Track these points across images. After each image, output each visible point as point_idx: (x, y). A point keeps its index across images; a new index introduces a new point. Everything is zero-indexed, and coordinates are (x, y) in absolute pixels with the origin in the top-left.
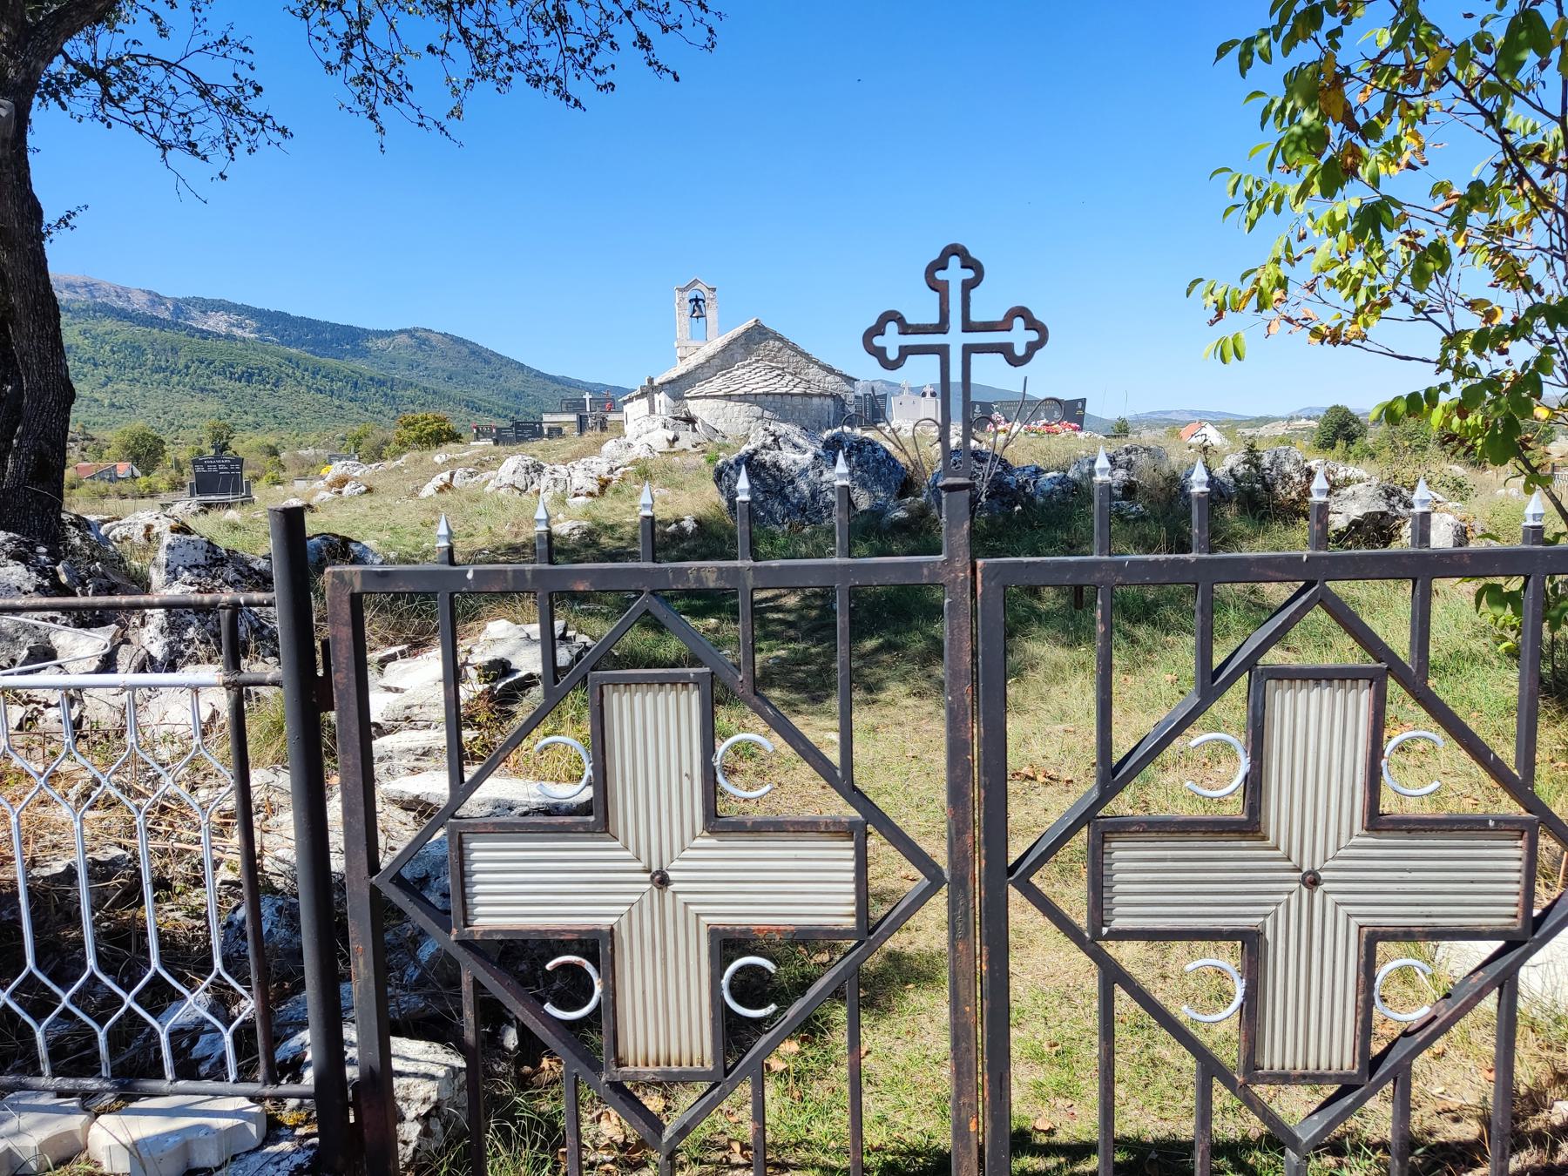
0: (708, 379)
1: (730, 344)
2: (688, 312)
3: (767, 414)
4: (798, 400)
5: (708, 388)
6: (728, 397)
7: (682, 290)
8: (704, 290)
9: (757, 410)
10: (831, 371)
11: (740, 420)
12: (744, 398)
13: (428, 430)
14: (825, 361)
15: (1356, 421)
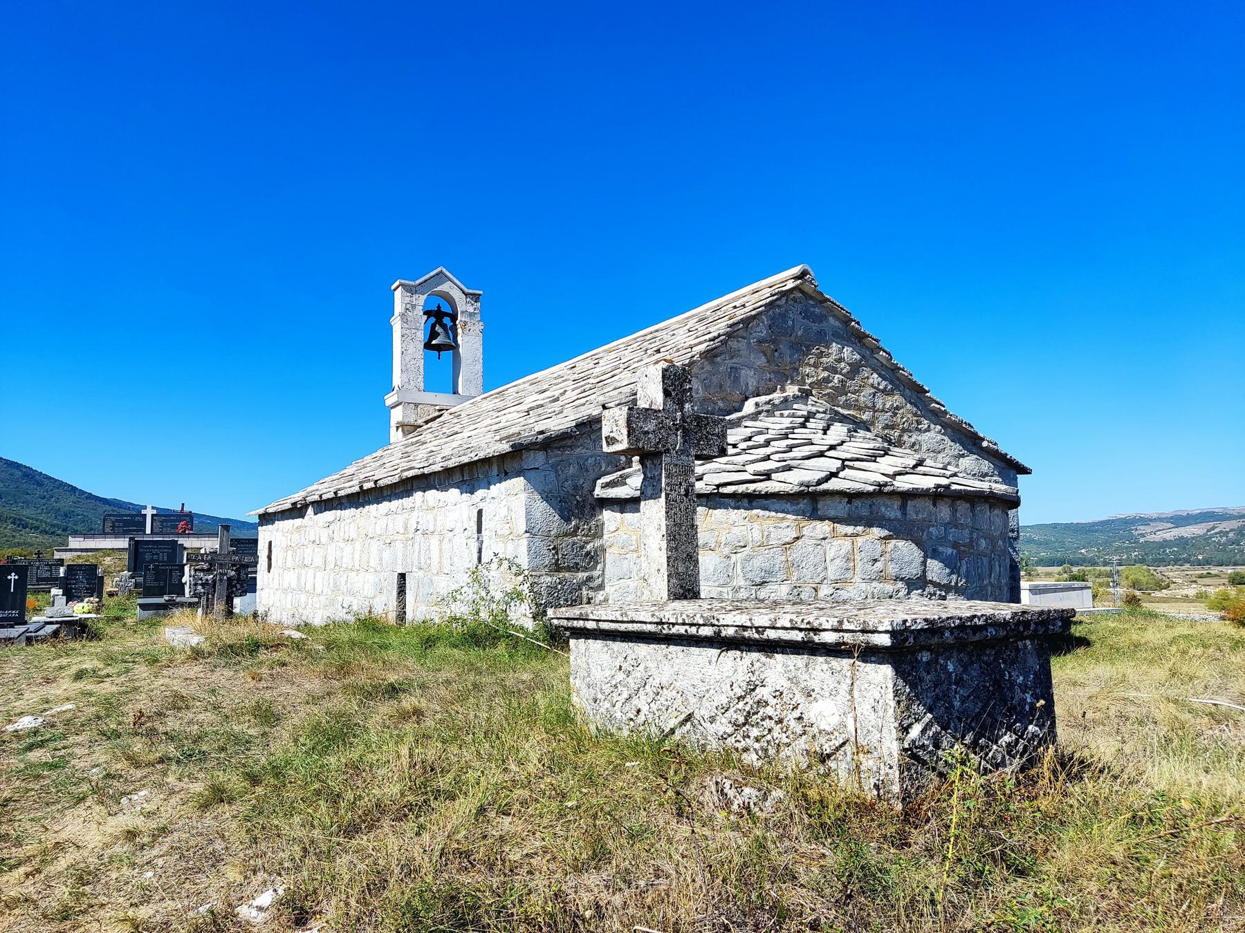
1: (734, 332)
2: (421, 336)
3: (936, 570)
6: (810, 502)
8: (457, 295)
9: (907, 553)
10: (969, 440)
12: (863, 508)
14: (958, 410)
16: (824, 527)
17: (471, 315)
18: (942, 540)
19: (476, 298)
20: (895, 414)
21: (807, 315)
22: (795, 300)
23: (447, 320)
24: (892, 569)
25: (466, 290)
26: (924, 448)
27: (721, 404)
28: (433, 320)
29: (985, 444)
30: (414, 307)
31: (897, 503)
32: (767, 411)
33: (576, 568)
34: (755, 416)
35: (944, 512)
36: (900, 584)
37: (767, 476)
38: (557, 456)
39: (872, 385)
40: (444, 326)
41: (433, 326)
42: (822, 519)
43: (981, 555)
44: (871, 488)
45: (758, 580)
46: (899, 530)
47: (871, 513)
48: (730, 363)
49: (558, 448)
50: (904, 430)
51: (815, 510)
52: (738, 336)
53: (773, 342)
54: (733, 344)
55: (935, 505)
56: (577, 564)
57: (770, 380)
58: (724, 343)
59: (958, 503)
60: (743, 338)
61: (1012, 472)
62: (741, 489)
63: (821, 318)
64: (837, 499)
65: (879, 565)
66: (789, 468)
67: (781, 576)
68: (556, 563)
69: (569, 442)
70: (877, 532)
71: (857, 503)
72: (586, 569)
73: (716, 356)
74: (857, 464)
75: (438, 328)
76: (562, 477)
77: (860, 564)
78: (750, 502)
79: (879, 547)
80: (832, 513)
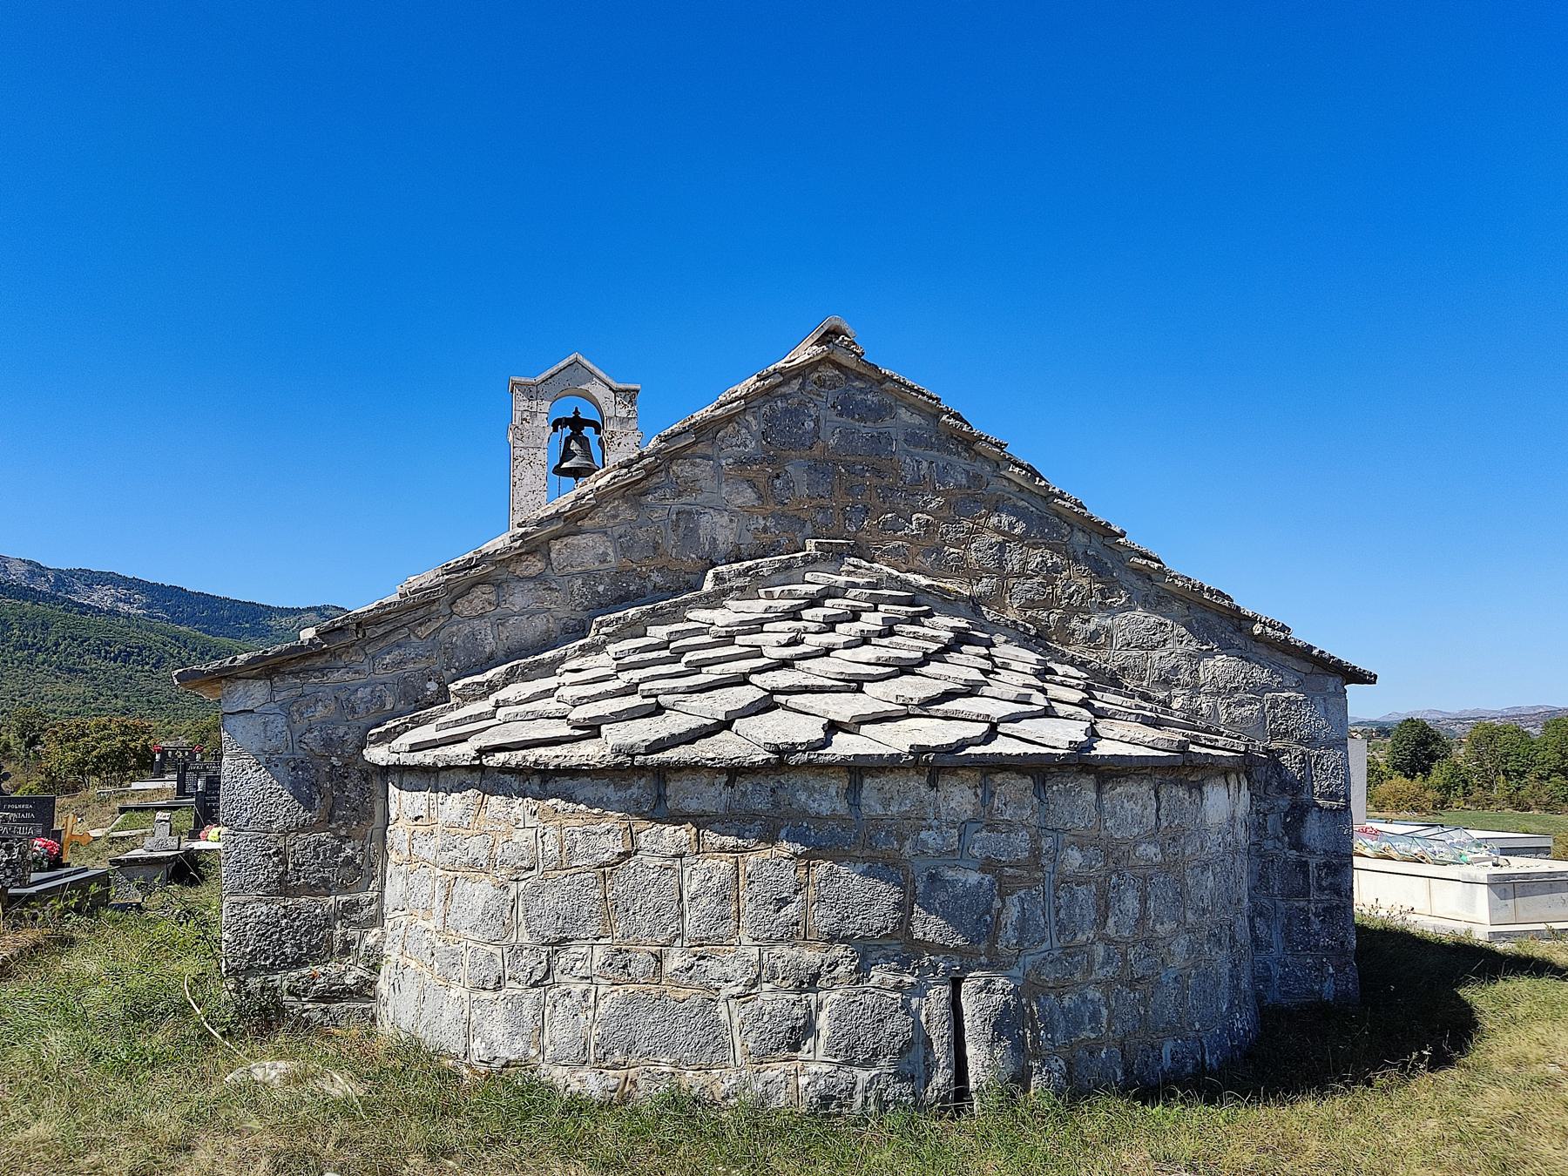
0: (529, 656)
4: (1132, 804)
5: (518, 714)
7: (531, 392)
10: (1219, 622)
11: (731, 967)
12: (769, 799)
13: (103, 748)
14: (1193, 560)
15: (1437, 739)
16: (676, 836)
17: (623, 421)
18: (956, 856)
19: (630, 395)
20: (1051, 582)
21: (846, 407)
22: (821, 383)
23: (588, 431)
24: (822, 919)
25: (615, 385)
26: (1118, 640)
27: (656, 578)
28: (568, 431)
29: (1257, 629)
30: (534, 414)
31: (836, 785)
32: (742, 589)
33: (325, 887)
34: (714, 601)
35: (959, 797)
36: (839, 951)
37: (592, 729)
38: (295, 686)
39: (997, 530)
40: (584, 442)
41: (568, 441)
42: (677, 819)
43: (1068, 882)
44: (760, 756)
45: (551, 934)
46: (821, 843)
47: (776, 805)
48: (676, 504)
49: (295, 674)
50: (1072, 611)
51: (661, 798)
52: (694, 455)
53: (772, 461)
54: (681, 469)
55: (933, 784)
56: (325, 880)
57: (765, 529)
58: (650, 472)
59: (998, 778)
60: (708, 458)
61: (1331, 683)
62: (515, 758)
63: (880, 412)
64: (705, 778)
65: (790, 910)
66: (659, 710)
67: (593, 928)
68: (281, 880)
69: (319, 662)
70: (786, 848)
71: (745, 784)
72: (345, 889)
73: (645, 493)
74: (795, 700)
75: (574, 446)
76: (301, 725)
77: (751, 907)
78: (544, 782)
79: (790, 875)
80: (693, 806)
